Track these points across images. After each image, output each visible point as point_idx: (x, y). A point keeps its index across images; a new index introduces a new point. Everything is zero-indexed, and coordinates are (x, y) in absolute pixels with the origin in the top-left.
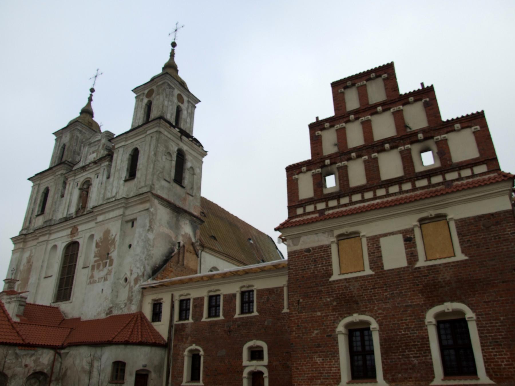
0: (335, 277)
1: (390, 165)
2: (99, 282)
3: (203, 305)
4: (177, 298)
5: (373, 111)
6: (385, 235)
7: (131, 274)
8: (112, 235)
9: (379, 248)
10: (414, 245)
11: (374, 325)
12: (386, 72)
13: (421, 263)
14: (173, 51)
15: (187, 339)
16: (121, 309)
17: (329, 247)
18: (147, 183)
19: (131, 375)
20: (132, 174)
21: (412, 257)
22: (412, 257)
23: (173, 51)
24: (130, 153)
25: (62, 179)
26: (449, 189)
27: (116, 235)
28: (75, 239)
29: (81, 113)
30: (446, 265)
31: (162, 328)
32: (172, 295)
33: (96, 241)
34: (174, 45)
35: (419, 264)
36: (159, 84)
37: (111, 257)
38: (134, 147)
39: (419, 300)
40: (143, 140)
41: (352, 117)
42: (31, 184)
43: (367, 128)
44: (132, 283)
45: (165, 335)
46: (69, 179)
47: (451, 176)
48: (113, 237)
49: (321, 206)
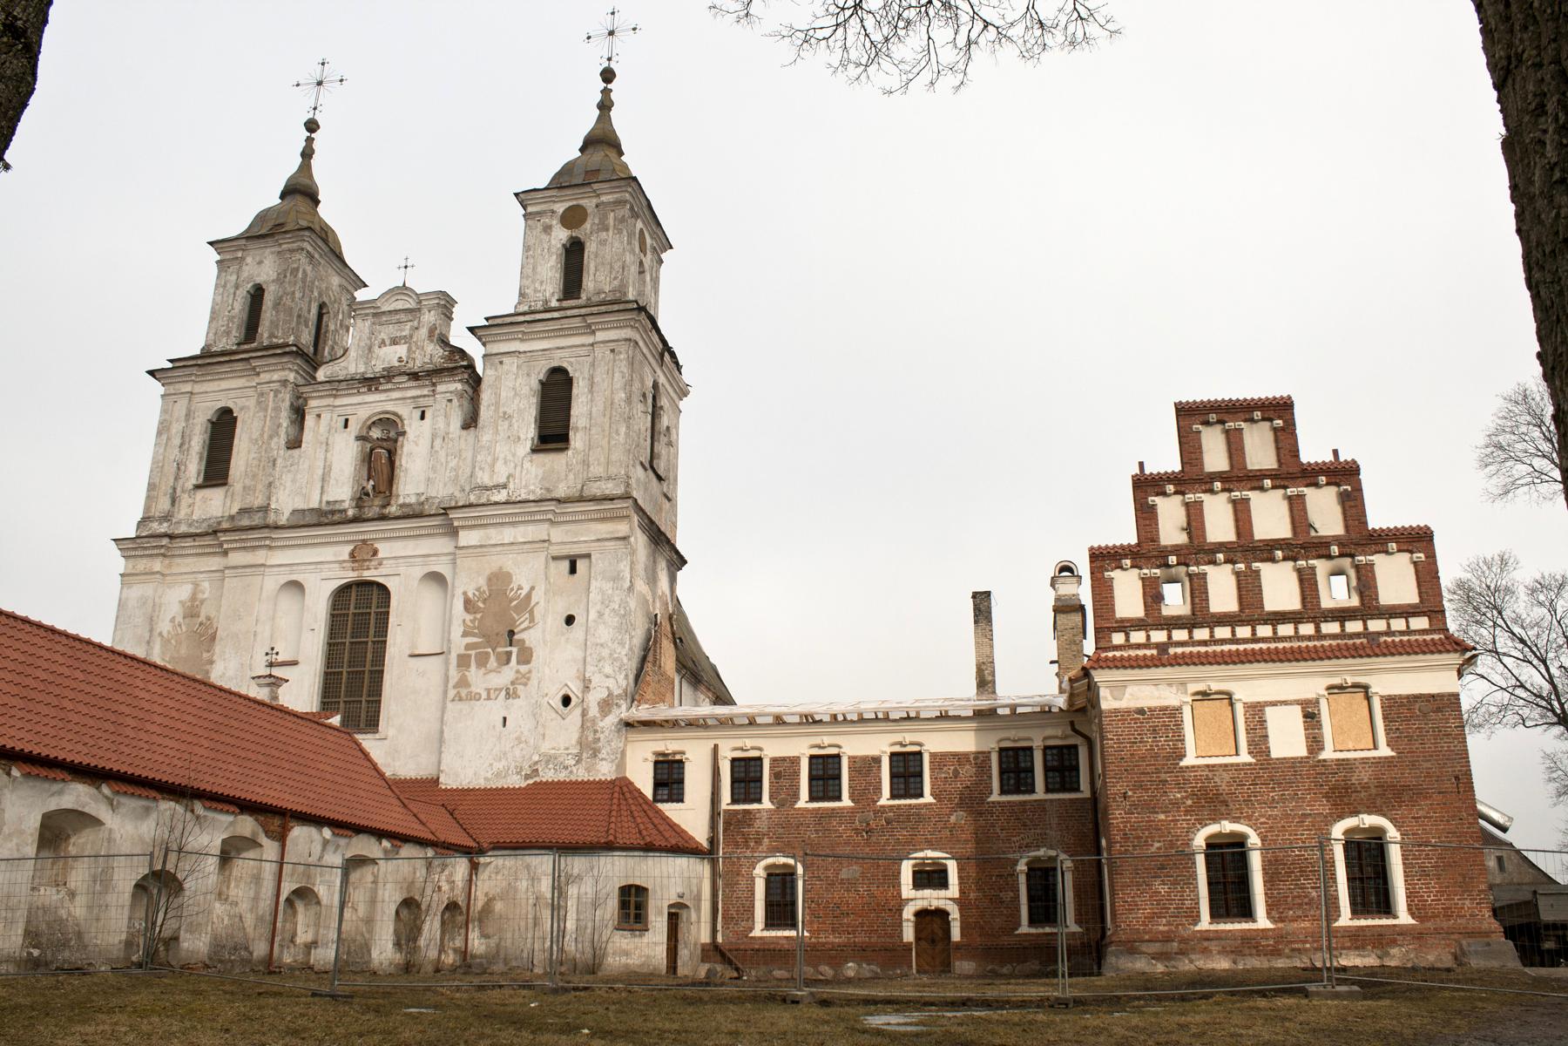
0: (1190, 760)
1: (1279, 587)
2: (489, 698)
3: (797, 774)
4: (727, 755)
5: (1256, 484)
6: (1274, 704)
7: (587, 688)
8: (520, 588)
9: (1263, 722)
10: (1319, 726)
11: (1254, 839)
12: (1279, 411)
13: (1328, 754)
14: (606, 92)
15: (758, 842)
16: (566, 768)
17: (1179, 709)
18: (613, 470)
19: (660, 913)
20: (553, 434)
21: (1315, 743)
22: (1315, 743)
23: (606, 92)
24: (541, 377)
25: (286, 398)
26: (1373, 647)
27: (533, 588)
28: (368, 575)
29: (283, 196)
30: (1364, 761)
31: (691, 815)
32: (716, 747)
33: (465, 593)
34: (608, 75)
35: (1324, 755)
36: (604, 198)
37: (523, 641)
38: (555, 364)
39: (1323, 807)
40: (582, 351)
41: (1218, 485)
42: (157, 388)
43: (1241, 512)
44: (594, 711)
45: (700, 834)
46: (312, 403)
47: (1376, 625)
48: (524, 592)
49: (1159, 636)
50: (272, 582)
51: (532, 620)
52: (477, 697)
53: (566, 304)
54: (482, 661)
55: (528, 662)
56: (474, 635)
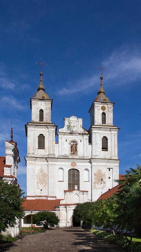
2: (99, 189)
8: (103, 173)
20: (105, 148)
28: (75, 168)
33: (94, 173)
48: (104, 173)
50: (57, 168)
51: (105, 177)
52: (97, 189)
53: (103, 124)
54: (98, 183)
55: (105, 184)
56: (96, 179)
